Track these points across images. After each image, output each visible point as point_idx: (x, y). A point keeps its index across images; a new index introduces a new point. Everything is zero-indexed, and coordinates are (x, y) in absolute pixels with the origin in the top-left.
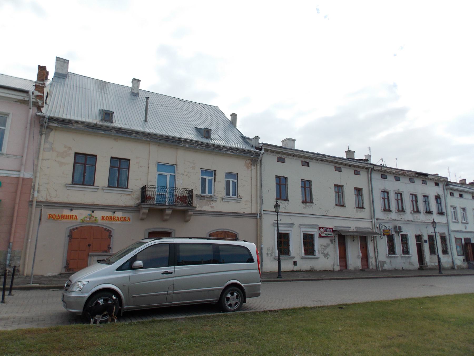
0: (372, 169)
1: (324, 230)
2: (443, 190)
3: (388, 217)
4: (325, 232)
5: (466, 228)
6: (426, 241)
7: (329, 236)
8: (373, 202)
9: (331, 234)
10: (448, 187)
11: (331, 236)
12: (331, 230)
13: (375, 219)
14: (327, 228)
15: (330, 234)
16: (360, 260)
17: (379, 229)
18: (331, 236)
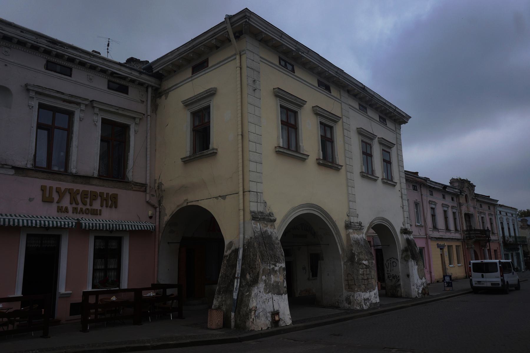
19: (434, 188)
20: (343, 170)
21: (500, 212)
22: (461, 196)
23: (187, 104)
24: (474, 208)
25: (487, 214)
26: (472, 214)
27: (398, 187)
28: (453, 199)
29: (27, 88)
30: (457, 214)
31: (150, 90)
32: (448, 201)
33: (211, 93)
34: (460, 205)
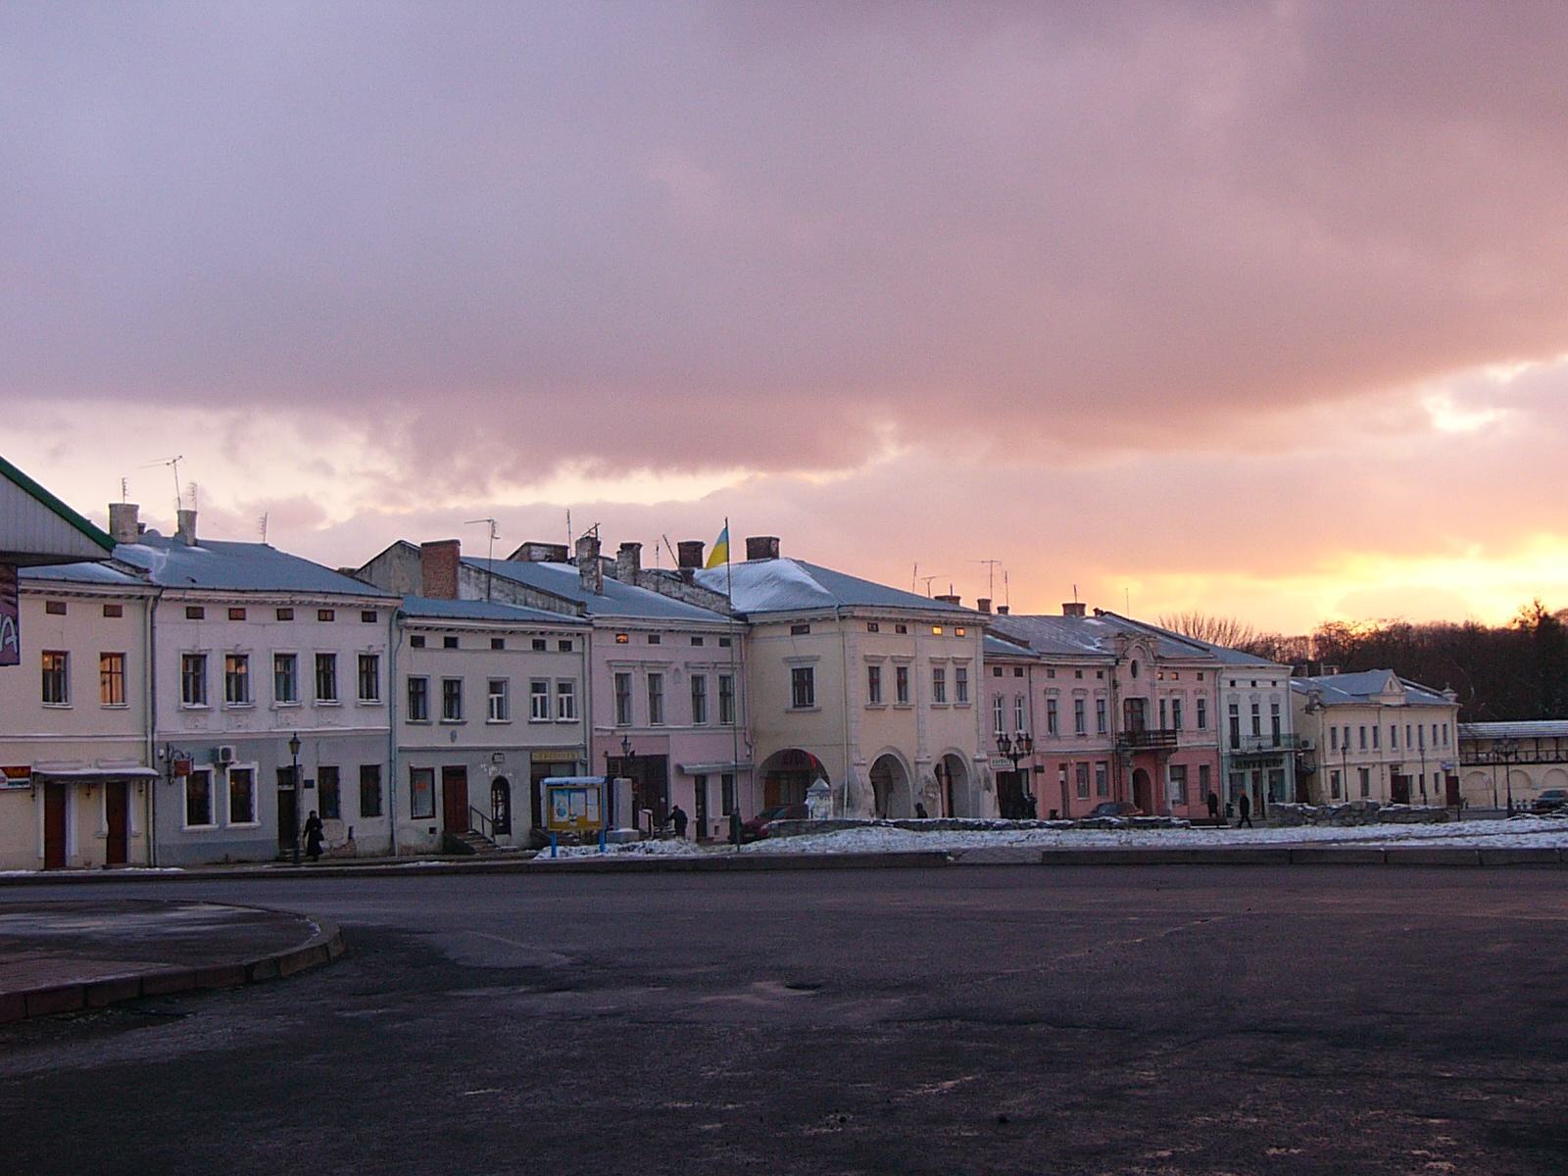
0: (156, 599)
1: (6, 773)
2: (387, 633)
3: (197, 724)
4: (9, 777)
5: (453, 737)
6: (309, 784)
7: (19, 786)
8: (153, 688)
9: (26, 783)
10: (402, 622)
11: (25, 786)
12: (26, 771)
13: (155, 735)
14: (16, 768)
15: (20, 783)
16: (103, 843)
17: (165, 759)
18: (25, 786)
19: (1056, 665)
20: (914, 709)
21: (1233, 683)
22: (1117, 667)
23: (787, 660)
24: (1153, 685)
25: (1190, 693)
26: (1146, 699)
27: (973, 708)
28: (1100, 675)
29: (687, 665)
30: (1107, 703)
31: (743, 637)
32: (1089, 680)
33: (817, 659)
34: (1115, 685)
